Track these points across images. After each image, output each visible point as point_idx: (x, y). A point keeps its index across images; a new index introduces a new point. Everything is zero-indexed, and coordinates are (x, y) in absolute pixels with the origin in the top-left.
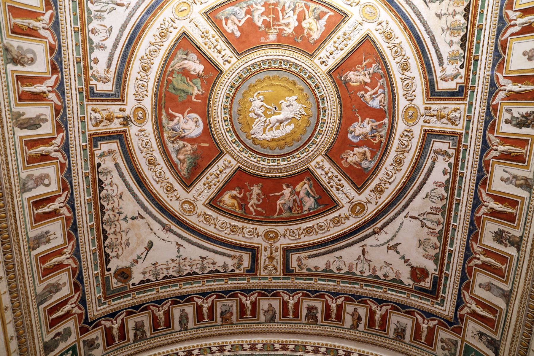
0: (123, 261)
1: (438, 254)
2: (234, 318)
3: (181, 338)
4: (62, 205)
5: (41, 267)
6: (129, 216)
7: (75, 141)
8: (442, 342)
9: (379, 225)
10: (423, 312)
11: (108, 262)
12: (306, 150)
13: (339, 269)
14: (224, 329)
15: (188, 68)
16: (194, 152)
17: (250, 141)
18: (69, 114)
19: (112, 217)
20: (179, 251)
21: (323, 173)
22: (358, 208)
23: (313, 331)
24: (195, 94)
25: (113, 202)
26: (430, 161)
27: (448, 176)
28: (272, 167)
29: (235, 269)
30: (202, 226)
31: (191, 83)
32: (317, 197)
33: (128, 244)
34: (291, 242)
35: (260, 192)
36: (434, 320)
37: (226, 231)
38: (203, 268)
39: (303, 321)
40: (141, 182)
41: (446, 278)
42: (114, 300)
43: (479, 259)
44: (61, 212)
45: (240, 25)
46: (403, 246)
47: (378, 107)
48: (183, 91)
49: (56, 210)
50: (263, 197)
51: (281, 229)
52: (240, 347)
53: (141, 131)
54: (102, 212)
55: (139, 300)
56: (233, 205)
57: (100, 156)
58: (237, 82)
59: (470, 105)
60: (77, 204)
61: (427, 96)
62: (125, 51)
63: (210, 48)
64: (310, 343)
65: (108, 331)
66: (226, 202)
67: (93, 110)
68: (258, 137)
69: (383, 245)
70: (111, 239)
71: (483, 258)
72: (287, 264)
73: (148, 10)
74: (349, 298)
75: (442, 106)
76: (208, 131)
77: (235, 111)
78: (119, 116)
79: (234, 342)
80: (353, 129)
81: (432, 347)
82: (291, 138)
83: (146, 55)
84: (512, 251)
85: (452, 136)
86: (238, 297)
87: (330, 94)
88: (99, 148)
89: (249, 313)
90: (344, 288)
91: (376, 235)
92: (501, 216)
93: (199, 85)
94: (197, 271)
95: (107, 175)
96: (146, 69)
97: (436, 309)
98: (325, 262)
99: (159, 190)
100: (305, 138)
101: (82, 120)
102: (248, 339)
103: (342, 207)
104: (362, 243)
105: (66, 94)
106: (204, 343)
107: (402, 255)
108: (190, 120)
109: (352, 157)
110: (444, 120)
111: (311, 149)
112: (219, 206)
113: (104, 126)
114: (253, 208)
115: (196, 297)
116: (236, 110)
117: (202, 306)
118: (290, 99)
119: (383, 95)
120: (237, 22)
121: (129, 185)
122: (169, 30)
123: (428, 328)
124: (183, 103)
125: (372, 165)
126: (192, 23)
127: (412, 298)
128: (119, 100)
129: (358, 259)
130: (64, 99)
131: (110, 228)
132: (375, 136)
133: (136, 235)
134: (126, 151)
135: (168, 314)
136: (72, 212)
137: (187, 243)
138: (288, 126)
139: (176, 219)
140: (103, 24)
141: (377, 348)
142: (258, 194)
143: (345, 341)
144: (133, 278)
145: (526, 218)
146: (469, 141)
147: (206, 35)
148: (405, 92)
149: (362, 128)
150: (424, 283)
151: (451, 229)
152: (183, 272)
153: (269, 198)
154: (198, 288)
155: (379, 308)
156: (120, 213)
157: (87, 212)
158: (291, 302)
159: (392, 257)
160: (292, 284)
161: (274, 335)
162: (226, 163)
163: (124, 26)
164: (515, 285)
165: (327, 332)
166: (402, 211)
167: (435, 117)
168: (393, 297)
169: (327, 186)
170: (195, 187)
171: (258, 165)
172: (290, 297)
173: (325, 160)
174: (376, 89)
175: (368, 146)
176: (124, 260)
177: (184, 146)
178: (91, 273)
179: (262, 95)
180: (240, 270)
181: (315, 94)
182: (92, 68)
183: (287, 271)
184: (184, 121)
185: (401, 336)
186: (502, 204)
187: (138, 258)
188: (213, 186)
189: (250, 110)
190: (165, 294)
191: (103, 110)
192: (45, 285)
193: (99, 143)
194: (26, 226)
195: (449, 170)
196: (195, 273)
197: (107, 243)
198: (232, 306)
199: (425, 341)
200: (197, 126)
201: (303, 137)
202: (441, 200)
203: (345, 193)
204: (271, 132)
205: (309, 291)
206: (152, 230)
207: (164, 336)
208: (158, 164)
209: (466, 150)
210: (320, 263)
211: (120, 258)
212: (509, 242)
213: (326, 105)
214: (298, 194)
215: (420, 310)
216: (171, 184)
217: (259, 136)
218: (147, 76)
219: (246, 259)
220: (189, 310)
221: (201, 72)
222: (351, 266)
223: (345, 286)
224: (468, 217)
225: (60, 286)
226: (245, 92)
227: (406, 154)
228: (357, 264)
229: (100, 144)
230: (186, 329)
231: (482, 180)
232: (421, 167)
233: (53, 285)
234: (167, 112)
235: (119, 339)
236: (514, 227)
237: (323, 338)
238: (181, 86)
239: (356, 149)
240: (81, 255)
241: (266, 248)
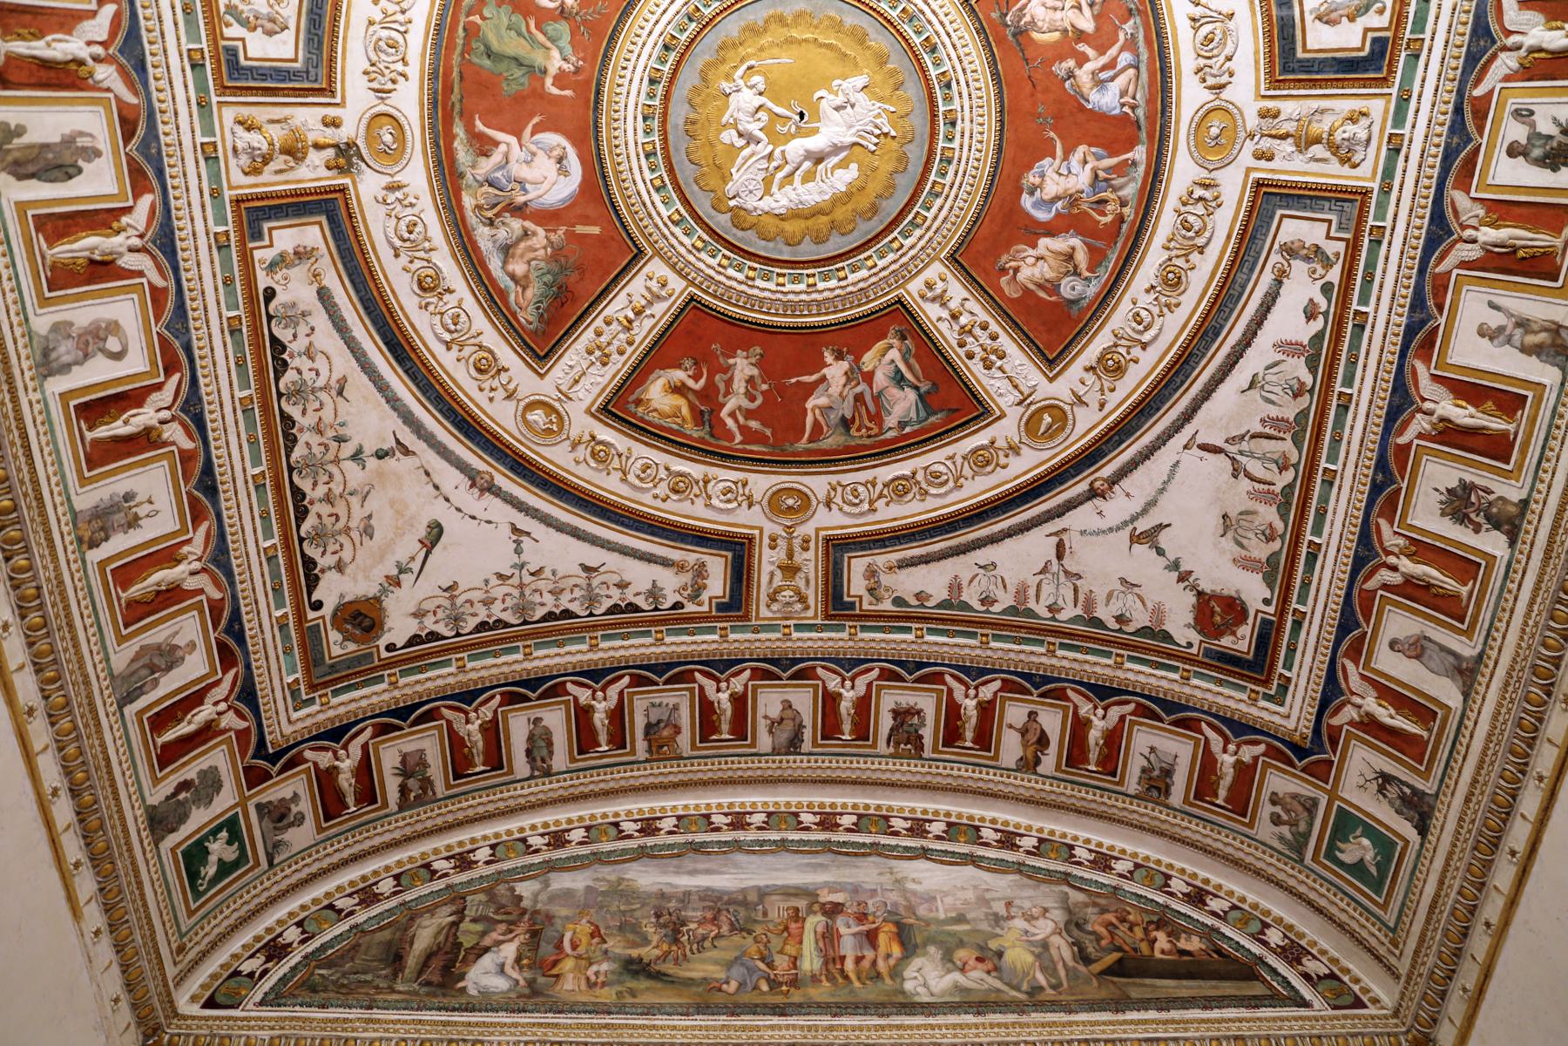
0: (355, 580)
1: (1276, 554)
2: (684, 740)
3: (532, 799)
4: (166, 414)
5: (119, 599)
6: (369, 449)
7: (192, 220)
8: (1274, 803)
9: (1107, 471)
10: (1224, 720)
11: (313, 581)
12: (895, 245)
13: (987, 601)
14: (656, 771)
16: (557, 254)
17: (724, 219)
18: (166, 134)
19: (317, 450)
20: (518, 551)
21: (945, 314)
22: (1047, 419)
23: (909, 777)
24: (553, 71)
25: (317, 405)
26: (1267, 278)
27: (1319, 324)
28: (791, 297)
29: (685, 602)
30: (586, 475)
31: (540, 37)
32: (924, 388)
33: (368, 531)
34: (848, 521)
35: (755, 372)
36: (1256, 743)
37: (657, 491)
38: (591, 600)
39: (882, 748)
40: (400, 347)
41: (1297, 625)
42: (336, 693)
43: (1394, 569)
44: (165, 436)
46: (1177, 532)
47: (1117, 111)
48: (518, 61)
49: (148, 430)
50: (765, 387)
51: (818, 484)
52: (702, 821)
53: (391, 188)
54: (286, 435)
55: (408, 691)
56: (676, 413)
57: (272, 267)
59: (1404, 101)
60: (211, 412)
61: (1270, 72)
64: (901, 809)
65: (326, 780)
66: (655, 404)
67: (240, 123)
68: (749, 206)
69: (1118, 529)
70: (319, 516)
71: (1406, 565)
72: (834, 587)
74: (1014, 682)
75: (1315, 104)
76: (597, 187)
77: (677, 126)
78: (322, 140)
79: (686, 807)
80: (1037, 181)
81: (1244, 816)
82: (850, 207)
84: (1493, 543)
85: (1338, 200)
86: (695, 681)
87: (969, 68)
88: (267, 242)
89: (725, 727)
90: (1000, 654)
91: (1098, 502)
92: (1470, 442)
94: (575, 607)
95: (297, 324)
97: (1264, 712)
98: (946, 580)
99: (454, 368)
100: (892, 207)
101: (209, 155)
102: (725, 801)
103: (999, 418)
104: (1057, 525)
105: (150, 70)
106: (598, 811)
107: (1172, 558)
108: (540, 153)
109: (1033, 265)
110: (1318, 150)
111: (908, 242)
112: (634, 415)
113: (281, 171)
114: (736, 421)
115: (573, 682)
116: (681, 122)
117: (592, 707)
118: (845, 85)
119: (1132, 71)
121: (365, 354)
123: (1239, 765)
124: (519, 99)
125: (1092, 290)
127: (1195, 682)
128: (319, 91)
129: (1044, 571)
130: (145, 84)
131: (315, 484)
132: (1104, 202)
133: (392, 503)
134: (350, 250)
135: (492, 731)
136: (196, 435)
137: (542, 526)
138: (839, 172)
139: (507, 455)
141: (1091, 822)
142: (750, 381)
143: (1000, 803)
144: (390, 630)
145: (1544, 447)
146: (1390, 216)
148: (1202, 62)
149: (1063, 176)
150: (1231, 638)
151: (1319, 481)
152: (533, 610)
153: (781, 389)
154: (579, 657)
155: (1100, 712)
156: (340, 440)
157: (244, 436)
158: (849, 696)
159: (1144, 565)
160: (851, 644)
161: (799, 789)
162: (654, 285)
164: (1495, 640)
165: (949, 780)
166: (1176, 427)
167: (1290, 140)
168: (1142, 678)
169: (957, 355)
170: (562, 361)
171: (750, 291)
172: (844, 680)
173: (950, 277)
174: (1113, 51)
175: (1080, 232)
176: (360, 576)
177: (526, 234)
178: (265, 616)
179: (758, 73)
180: (699, 604)
181: (924, 70)
183: (837, 605)
184: (523, 155)
185: (1159, 789)
186: (1476, 406)
187: (401, 572)
188: (615, 356)
189: (724, 120)
190: (484, 673)
192: (136, 648)
193: (266, 226)
194: (63, 476)
195: (1323, 304)
196: (567, 614)
197: (306, 527)
198: (676, 708)
199: (1226, 801)
200: (563, 171)
201: (884, 203)
202: (1295, 396)
203: (1008, 375)
204: (788, 188)
205: (899, 663)
206: (437, 487)
207: (484, 793)
208: (449, 291)
209: (1379, 242)
210: (933, 581)
211: (348, 571)
212: (1488, 518)
213: (956, 105)
214: (869, 377)
215: (1216, 716)
216: (491, 352)
217: (751, 202)
218: (403, 12)
219: (717, 570)
220: (555, 719)
222: (1021, 592)
223: (1002, 650)
224: (1371, 446)
225: (179, 653)
226: (709, 65)
227: (1195, 257)
228: (1039, 586)
229: (270, 230)
230: (548, 773)
231: (1421, 333)
232: (1241, 295)
233: (158, 649)
234: (470, 128)
235: (358, 801)
236: (1507, 474)
237: (939, 796)
238: (512, 45)
239: (1044, 242)
240: (234, 562)
241: (773, 539)
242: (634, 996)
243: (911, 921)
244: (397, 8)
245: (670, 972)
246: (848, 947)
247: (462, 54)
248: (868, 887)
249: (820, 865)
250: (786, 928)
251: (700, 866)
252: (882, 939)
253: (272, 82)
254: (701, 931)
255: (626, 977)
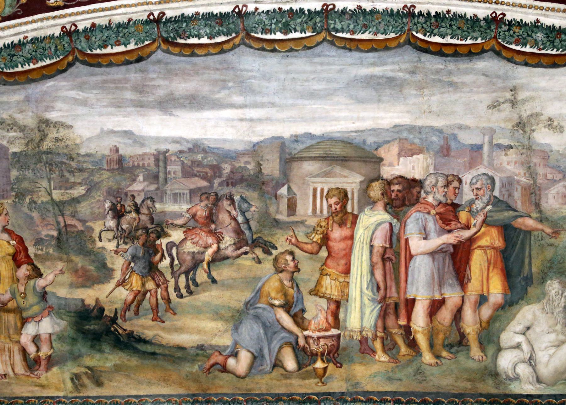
242: (99, 384)
243: (530, 223)
245: (149, 334)
246: (420, 282)
248: (468, 139)
249: (390, 81)
250: (326, 239)
251: (182, 87)
252: (478, 260)
254: (189, 247)
255: (82, 347)
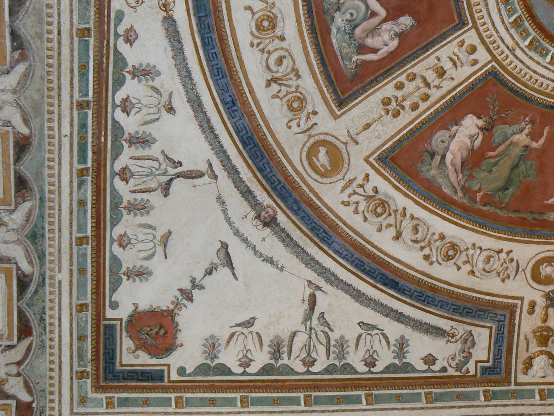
15: (465, 154)
45: (383, 13)
58: (528, 34)
62: (411, 297)
63: (426, 98)
73: (322, 240)
83: (422, 248)
93: (508, 129)
96: (452, 251)
120: (375, 21)
122: (371, 193)
126: (360, 138)
128: (513, 314)
140: (355, 341)
147: (394, 104)
163: (358, 296)
182: (444, 369)
191: (527, 350)
221: (480, 123)
238: (501, 172)
244: (464, 253)
247: (501, 209)
253: (503, 342)
